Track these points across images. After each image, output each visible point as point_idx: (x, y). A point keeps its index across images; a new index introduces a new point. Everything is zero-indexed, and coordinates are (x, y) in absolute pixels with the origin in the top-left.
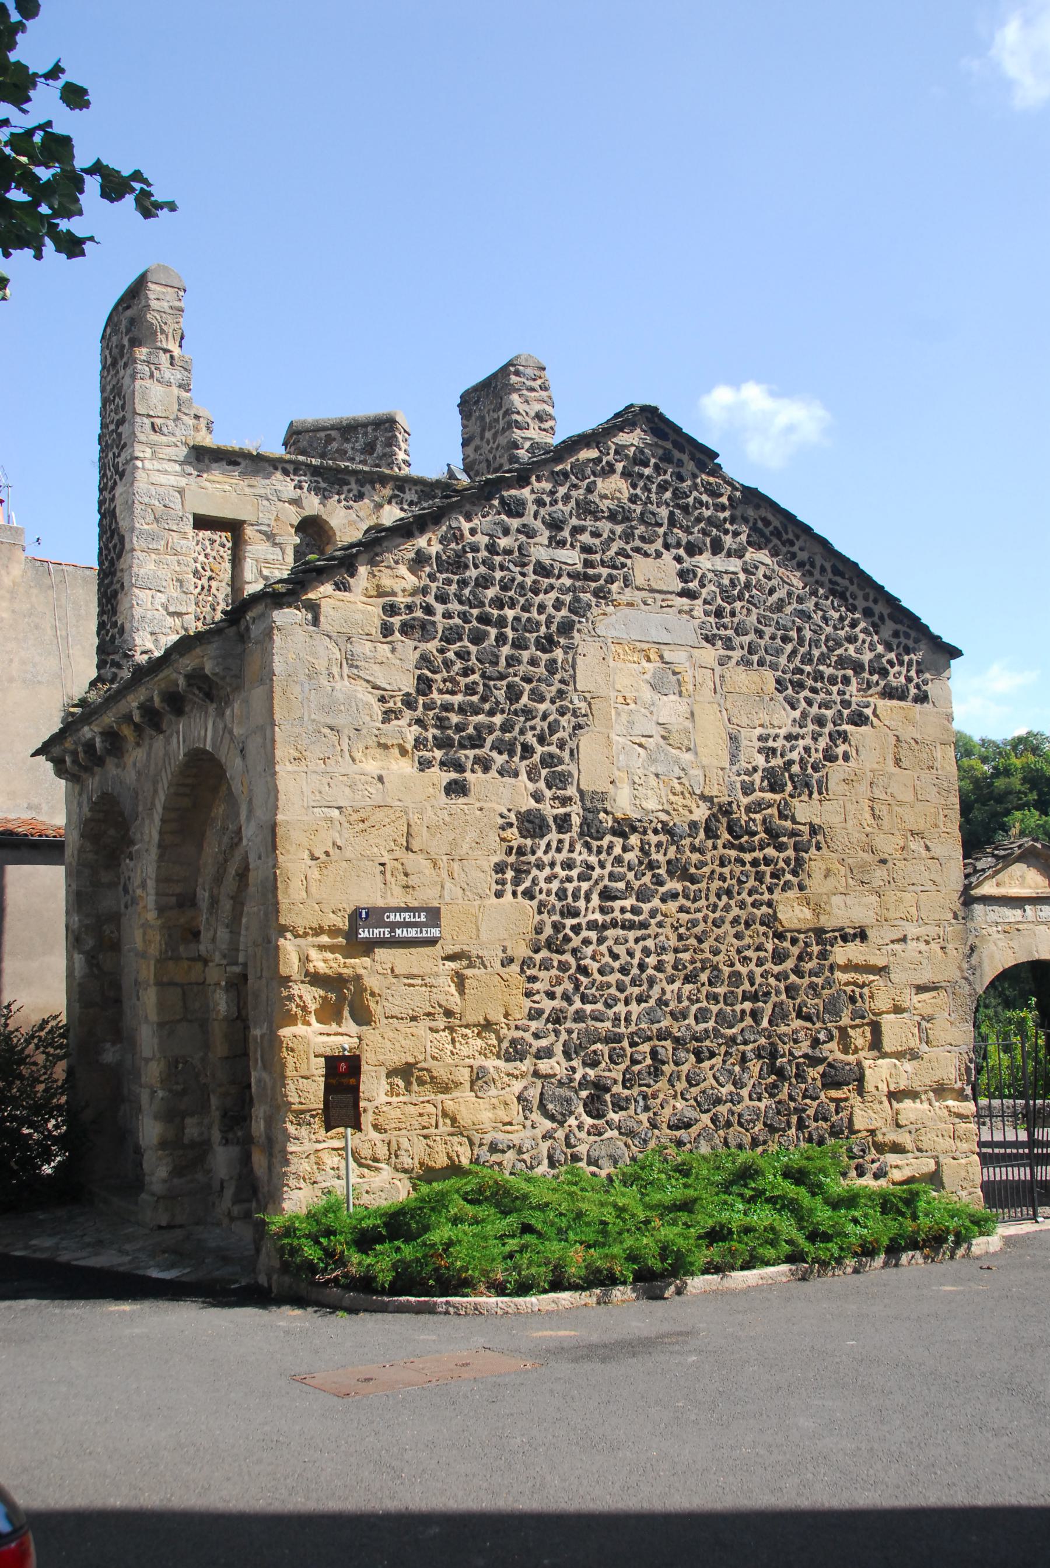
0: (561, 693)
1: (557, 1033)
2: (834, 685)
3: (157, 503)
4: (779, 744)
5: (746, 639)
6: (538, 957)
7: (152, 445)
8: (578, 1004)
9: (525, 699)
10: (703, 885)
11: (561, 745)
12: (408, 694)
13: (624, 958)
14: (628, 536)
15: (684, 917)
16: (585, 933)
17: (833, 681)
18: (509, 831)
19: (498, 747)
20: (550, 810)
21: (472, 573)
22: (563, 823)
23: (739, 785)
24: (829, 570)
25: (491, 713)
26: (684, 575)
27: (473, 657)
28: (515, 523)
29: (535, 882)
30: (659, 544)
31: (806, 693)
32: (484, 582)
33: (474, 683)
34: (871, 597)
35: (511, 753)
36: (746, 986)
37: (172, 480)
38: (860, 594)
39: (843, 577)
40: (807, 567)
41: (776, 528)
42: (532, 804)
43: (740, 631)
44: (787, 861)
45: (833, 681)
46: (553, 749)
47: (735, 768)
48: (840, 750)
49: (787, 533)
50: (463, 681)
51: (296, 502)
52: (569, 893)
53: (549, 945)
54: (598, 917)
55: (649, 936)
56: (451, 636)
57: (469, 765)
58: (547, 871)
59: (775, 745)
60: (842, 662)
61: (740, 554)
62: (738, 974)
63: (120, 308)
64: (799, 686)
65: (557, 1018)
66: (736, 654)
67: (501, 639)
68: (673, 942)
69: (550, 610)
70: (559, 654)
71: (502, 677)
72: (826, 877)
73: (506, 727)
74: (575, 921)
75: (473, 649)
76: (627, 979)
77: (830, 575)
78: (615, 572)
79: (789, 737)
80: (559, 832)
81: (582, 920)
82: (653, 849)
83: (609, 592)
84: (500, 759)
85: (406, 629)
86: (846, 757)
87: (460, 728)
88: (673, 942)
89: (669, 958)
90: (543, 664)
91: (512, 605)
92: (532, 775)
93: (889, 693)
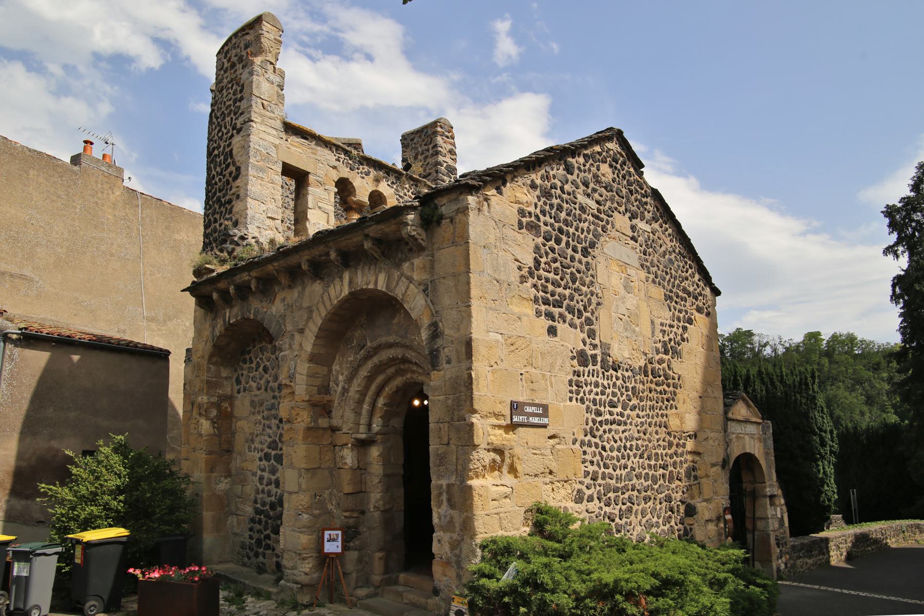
3: (263, 150)
7: (261, 115)
12: (530, 268)
37: (272, 139)
42: (581, 346)
51: (335, 168)
63: (240, 35)
80: (593, 365)
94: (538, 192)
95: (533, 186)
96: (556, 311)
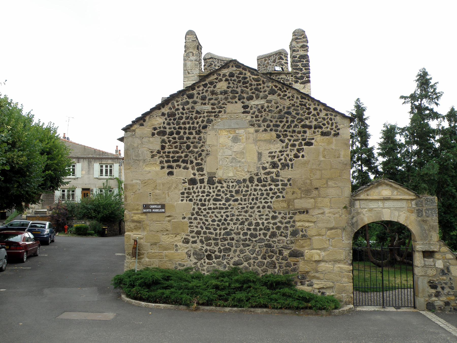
0: (202, 146)
1: (198, 237)
2: (300, 134)
4: (276, 154)
5: (266, 124)
6: (193, 217)
8: (205, 230)
9: (191, 148)
10: (247, 197)
11: (202, 160)
13: (220, 218)
14: (226, 99)
15: (240, 206)
16: (207, 211)
17: (299, 132)
18: (186, 183)
19: (184, 162)
20: (198, 178)
21: (177, 116)
22: (202, 181)
23: (261, 168)
24: (300, 98)
25: (182, 153)
26: (245, 107)
27: (177, 139)
28: (191, 101)
29: (193, 197)
30: (237, 100)
31: (289, 137)
32: (181, 118)
33: (177, 145)
34: (317, 104)
35: (187, 163)
36: (261, 226)
38: (312, 104)
39: (305, 99)
40: (291, 98)
41: (279, 88)
42: (192, 176)
43: (265, 120)
44: (279, 189)
45: (299, 132)
46: (199, 161)
47: (260, 162)
48: (300, 155)
49: (283, 89)
50: (174, 145)
52: (203, 200)
53: (197, 213)
54: (212, 206)
55: (228, 212)
56: (171, 134)
57: (175, 167)
58: (197, 194)
59: (275, 154)
60: (304, 126)
61: (265, 97)
62: (258, 223)
64: (286, 136)
65: (198, 233)
66: (262, 129)
67: (185, 133)
68: (237, 213)
69: (200, 123)
70: (202, 135)
71: (186, 143)
72: (293, 194)
73: (187, 156)
74: (204, 207)
75: (177, 136)
76: (220, 223)
77: (300, 99)
78: (221, 110)
79: (281, 152)
80: (200, 183)
81: (206, 207)
82: (230, 187)
83: (219, 116)
84: (183, 165)
85: (159, 134)
86: (303, 156)
87: (172, 157)
88: (237, 213)
89: (235, 218)
90: (197, 138)
91: (189, 123)
92: (193, 168)
93: (323, 134)
94: (166, 116)
95: (163, 114)
96: (174, 164)
